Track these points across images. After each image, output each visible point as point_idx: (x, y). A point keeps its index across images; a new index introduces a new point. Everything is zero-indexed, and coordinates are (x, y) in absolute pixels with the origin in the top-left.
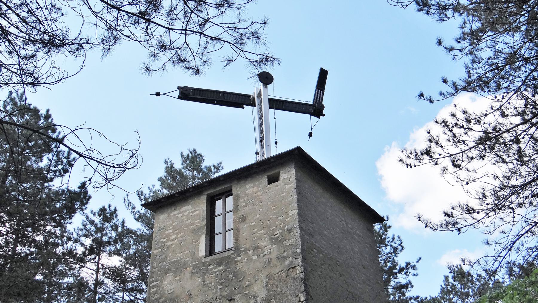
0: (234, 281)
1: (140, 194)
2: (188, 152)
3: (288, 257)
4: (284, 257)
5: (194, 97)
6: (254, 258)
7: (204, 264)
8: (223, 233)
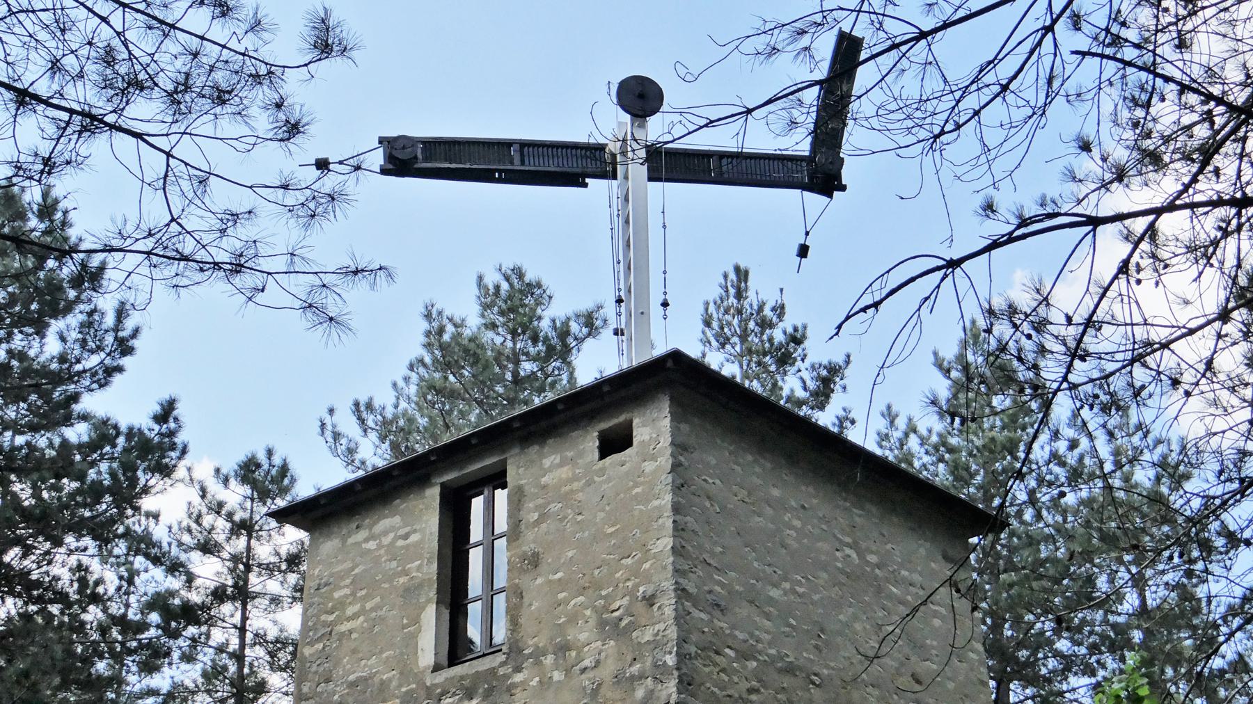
1: (361, 410)
2: (498, 278)
3: (642, 676)
5: (429, 165)
6: (557, 676)
7: (429, 691)
8: (484, 599)
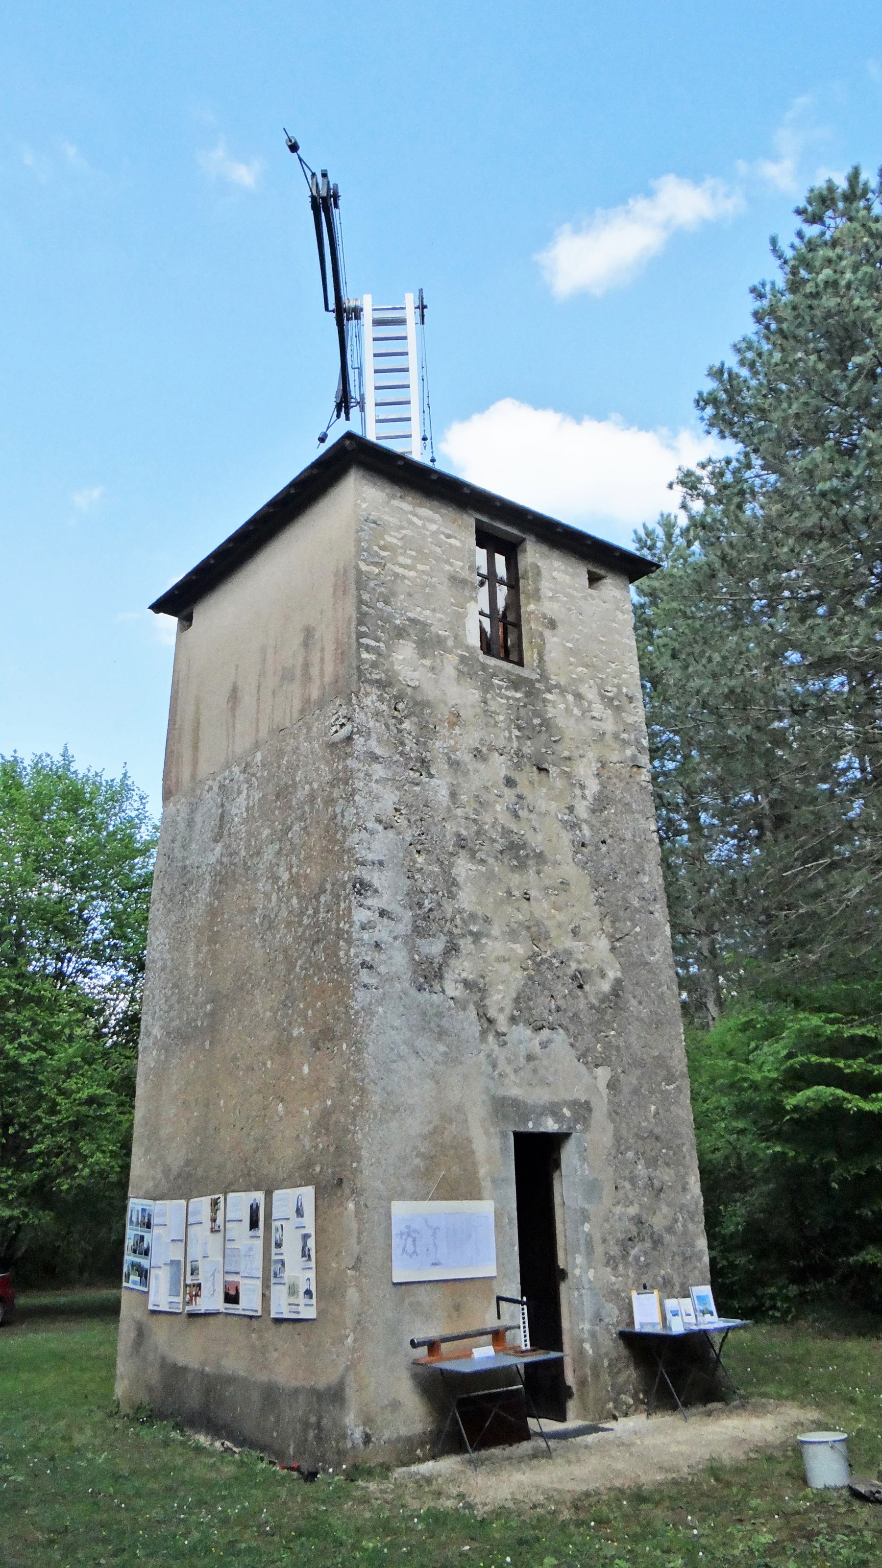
0: (544, 737)
4: (623, 740)
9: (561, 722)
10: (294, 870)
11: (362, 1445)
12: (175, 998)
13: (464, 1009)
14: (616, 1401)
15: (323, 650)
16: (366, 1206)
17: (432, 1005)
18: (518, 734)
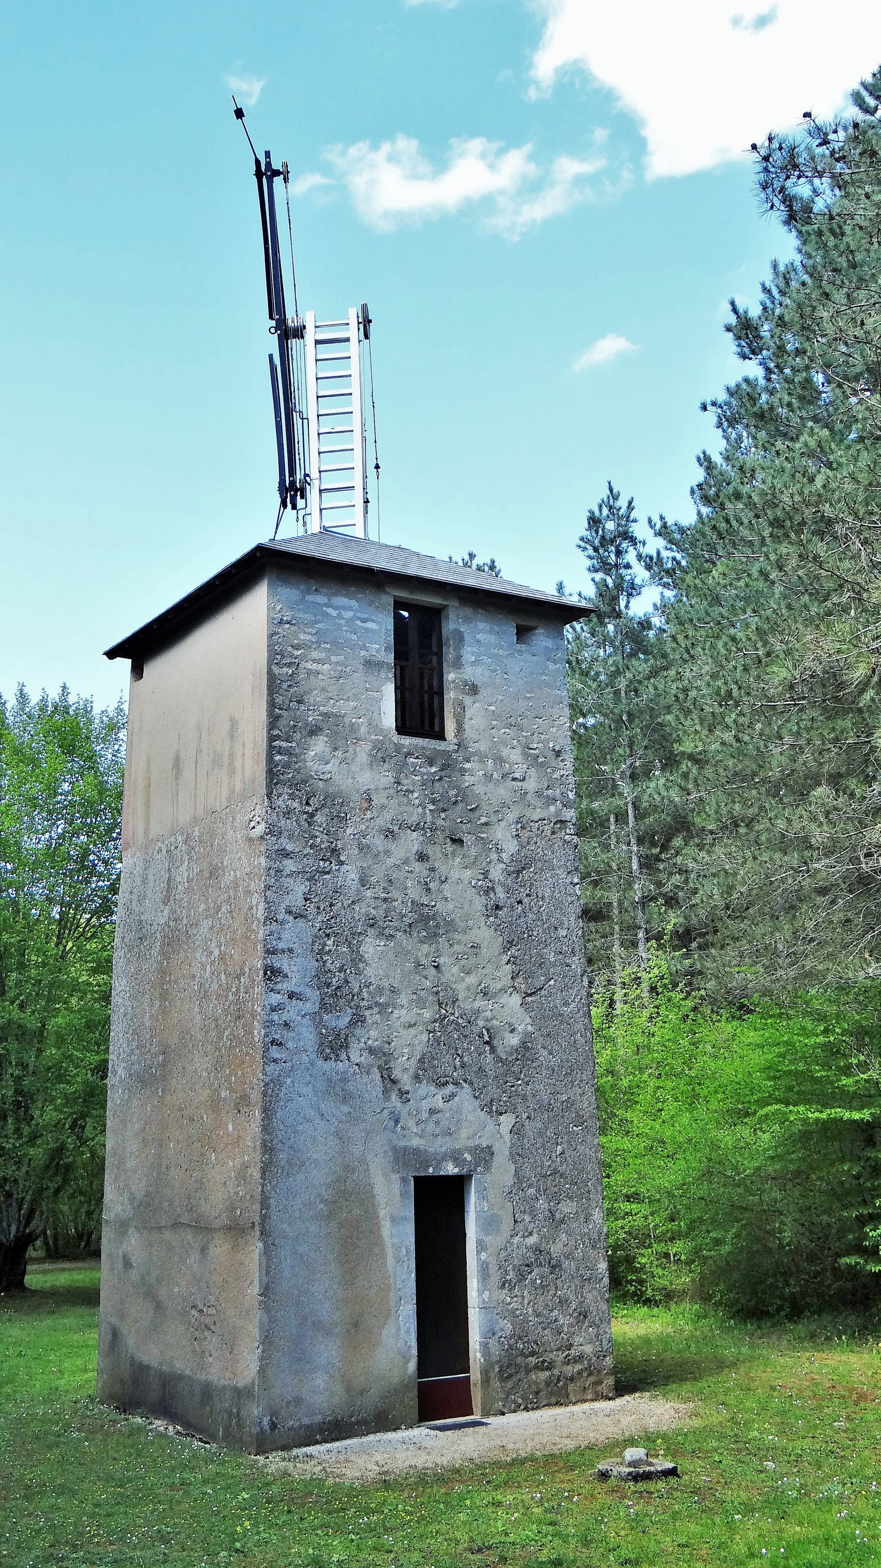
9: (479, 789)
10: (223, 948)
11: (269, 1431)
12: (135, 1044)
13: (368, 1073)
14: (505, 1400)
15: (244, 745)
16: (273, 1244)
17: (337, 1073)
18: (432, 807)
